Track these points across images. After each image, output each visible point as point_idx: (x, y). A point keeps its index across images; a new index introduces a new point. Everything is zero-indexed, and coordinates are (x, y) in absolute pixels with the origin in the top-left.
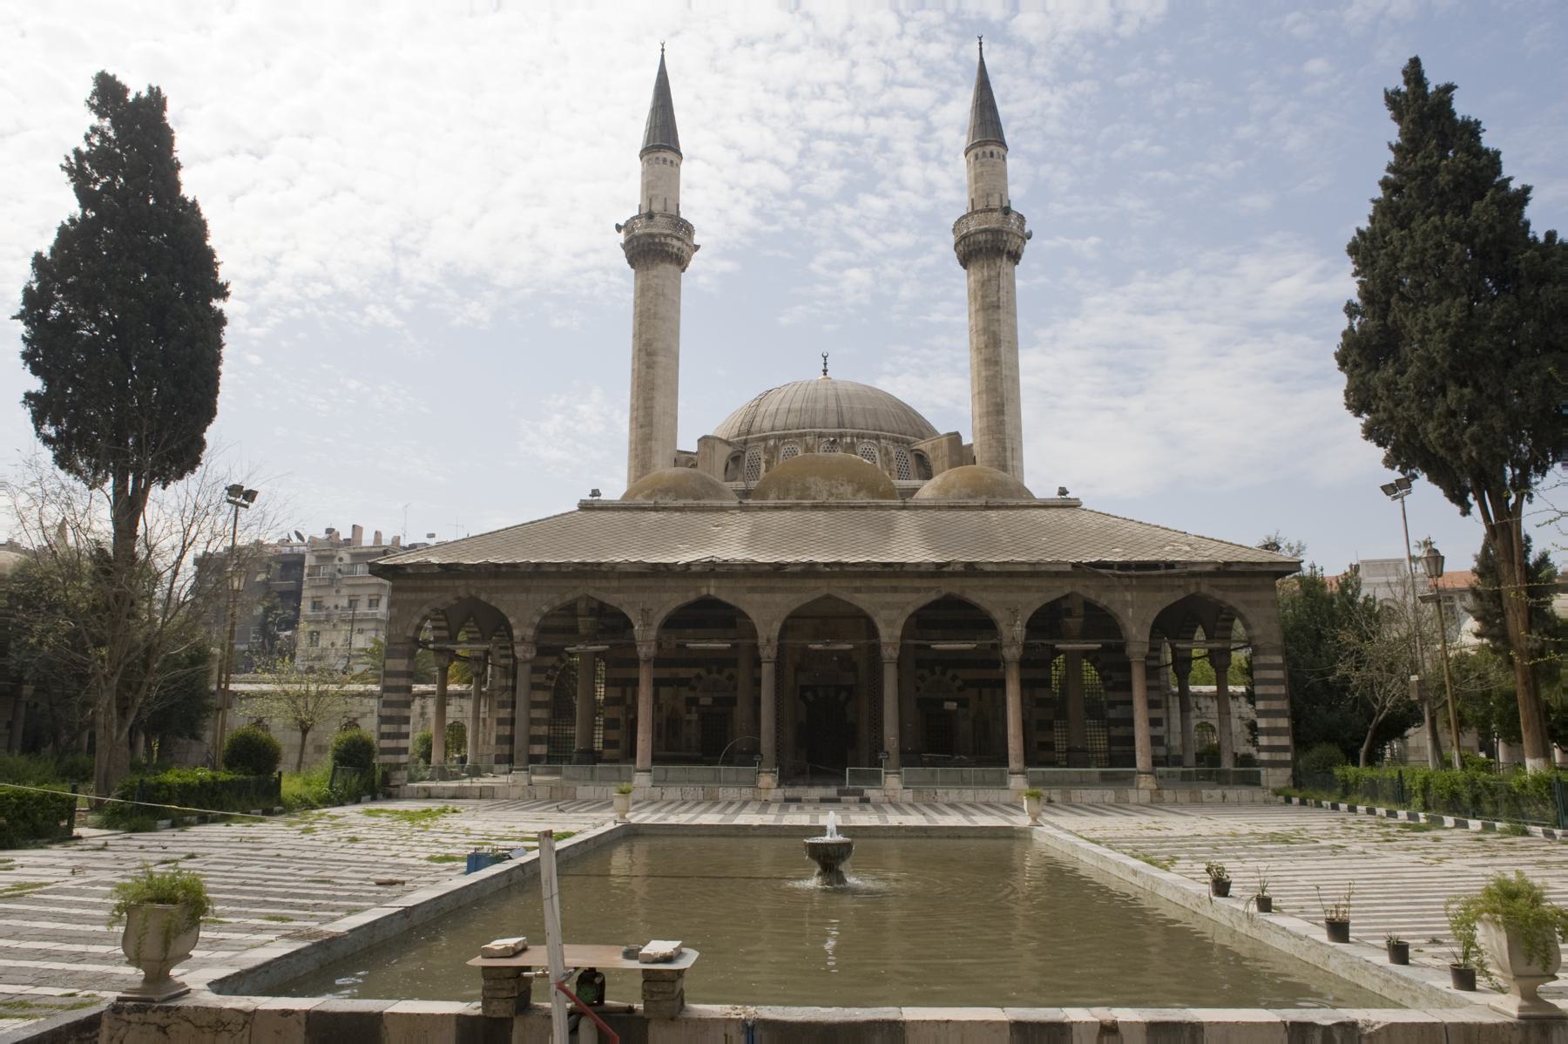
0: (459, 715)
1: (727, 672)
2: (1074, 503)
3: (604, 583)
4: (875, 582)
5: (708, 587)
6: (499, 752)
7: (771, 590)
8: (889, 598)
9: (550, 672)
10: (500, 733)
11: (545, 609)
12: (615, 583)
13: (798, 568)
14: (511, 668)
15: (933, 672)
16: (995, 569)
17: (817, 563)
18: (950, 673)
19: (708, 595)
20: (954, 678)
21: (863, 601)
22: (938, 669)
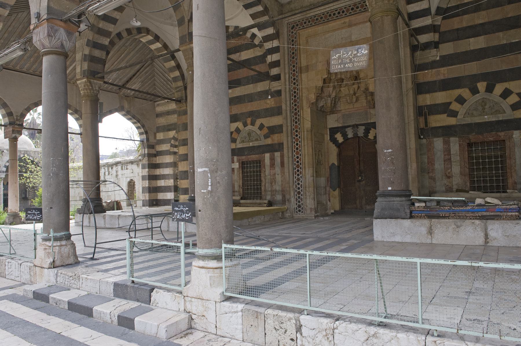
0: (132, 175)
1: (258, 122)
6: (144, 199)
9: (173, 142)
10: (144, 186)
14: (145, 141)
15: (475, 91)
18: (499, 89)
20: (506, 94)
22: (482, 86)
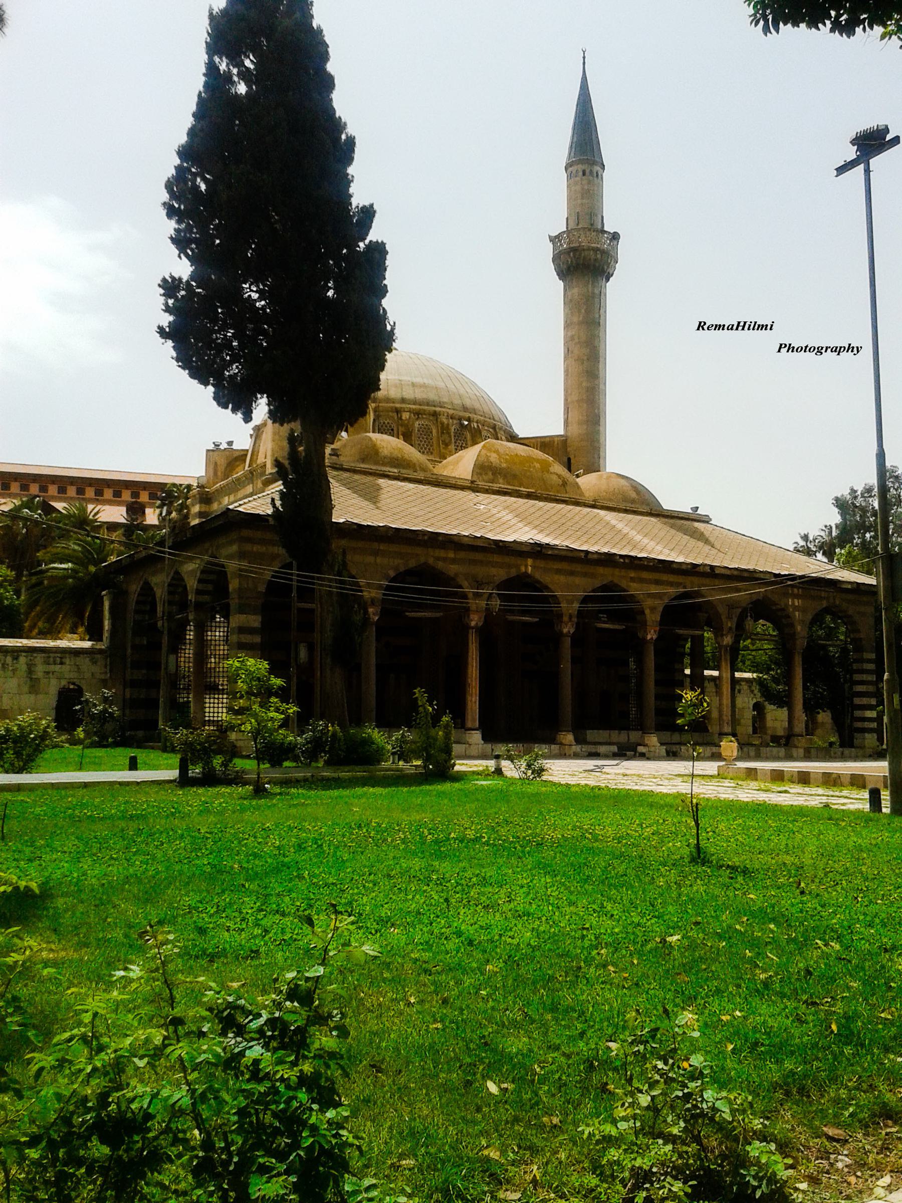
2: (704, 519)
3: (442, 553)
4: (645, 575)
5: (526, 566)
7: (572, 573)
8: (654, 589)
11: (392, 574)
12: (451, 555)
13: (595, 556)
16: (728, 572)
17: (615, 554)
19: (526, 572)
21: (635, 589)
